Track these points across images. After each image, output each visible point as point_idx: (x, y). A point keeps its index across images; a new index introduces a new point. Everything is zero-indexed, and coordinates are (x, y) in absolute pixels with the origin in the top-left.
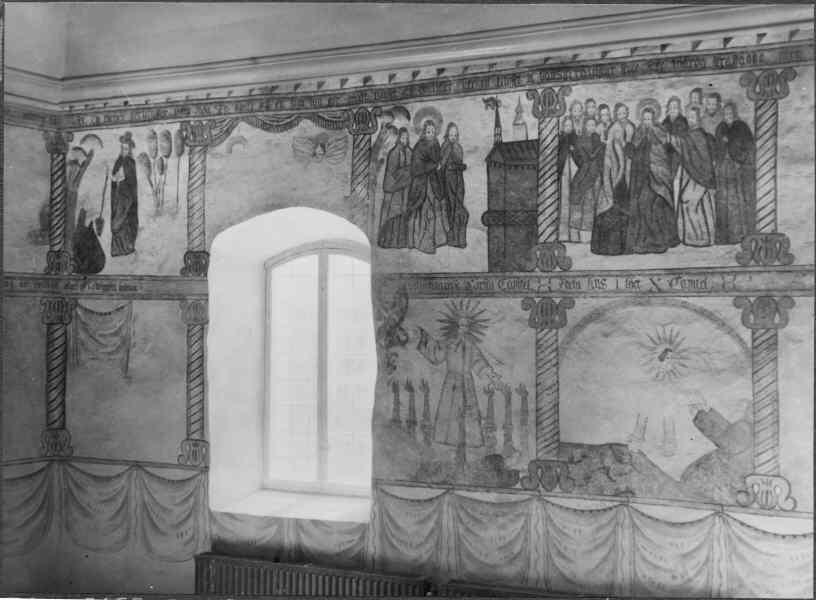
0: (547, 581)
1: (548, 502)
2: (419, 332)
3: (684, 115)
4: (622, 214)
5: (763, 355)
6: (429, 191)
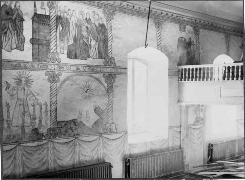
0: (55, 169)
1: (54, 142)
2: (6, 82)
3: (90, 18)
4: (75, 46)
5: (110, 90)
6: (10, 26)
